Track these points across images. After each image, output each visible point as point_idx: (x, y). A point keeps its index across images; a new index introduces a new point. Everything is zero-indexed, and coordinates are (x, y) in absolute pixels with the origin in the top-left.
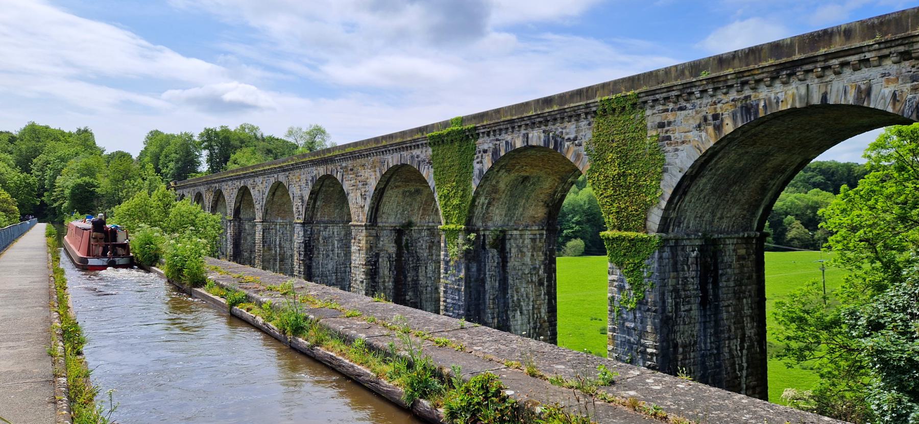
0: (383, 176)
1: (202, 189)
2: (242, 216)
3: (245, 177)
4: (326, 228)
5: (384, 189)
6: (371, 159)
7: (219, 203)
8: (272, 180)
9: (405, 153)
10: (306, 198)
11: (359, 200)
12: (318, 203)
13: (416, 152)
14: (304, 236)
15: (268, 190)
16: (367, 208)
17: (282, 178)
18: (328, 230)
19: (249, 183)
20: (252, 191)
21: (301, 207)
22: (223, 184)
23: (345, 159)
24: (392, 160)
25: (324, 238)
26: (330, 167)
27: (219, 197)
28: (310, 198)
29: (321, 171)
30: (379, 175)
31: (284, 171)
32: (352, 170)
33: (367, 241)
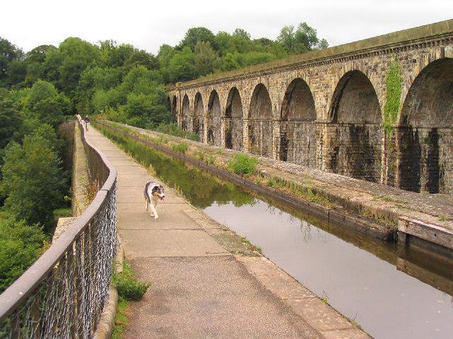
0: (341, 80)
1: (201, 90)
2: (233, 115)
3: (234, 80)
4: (299, 125)
5: (342, 91)
6: (331, 66)
7: (214, 105)
8: (256, 82)
9: (358, 62)
10: (282, 98)
11: (324, 102)
12: (292, 103)
13: (366, 60)
14: (281, 132)
15: (252, 91)
16: (328, 108)
17: (263, 81)
18: (301, 126)
19: (237, 84)
20: (240, 92)
21: (278, 106)
22: (218, 85)
23: (313, 65)
24: (348, 67)
25: (298, 133)
26: (301, 72)
27: (214, 95)
28: (285, 98)
29: (294, 74)
30: (337, 80)
31: (265, 74)
32: (317, 74)
33: (328, 136)
